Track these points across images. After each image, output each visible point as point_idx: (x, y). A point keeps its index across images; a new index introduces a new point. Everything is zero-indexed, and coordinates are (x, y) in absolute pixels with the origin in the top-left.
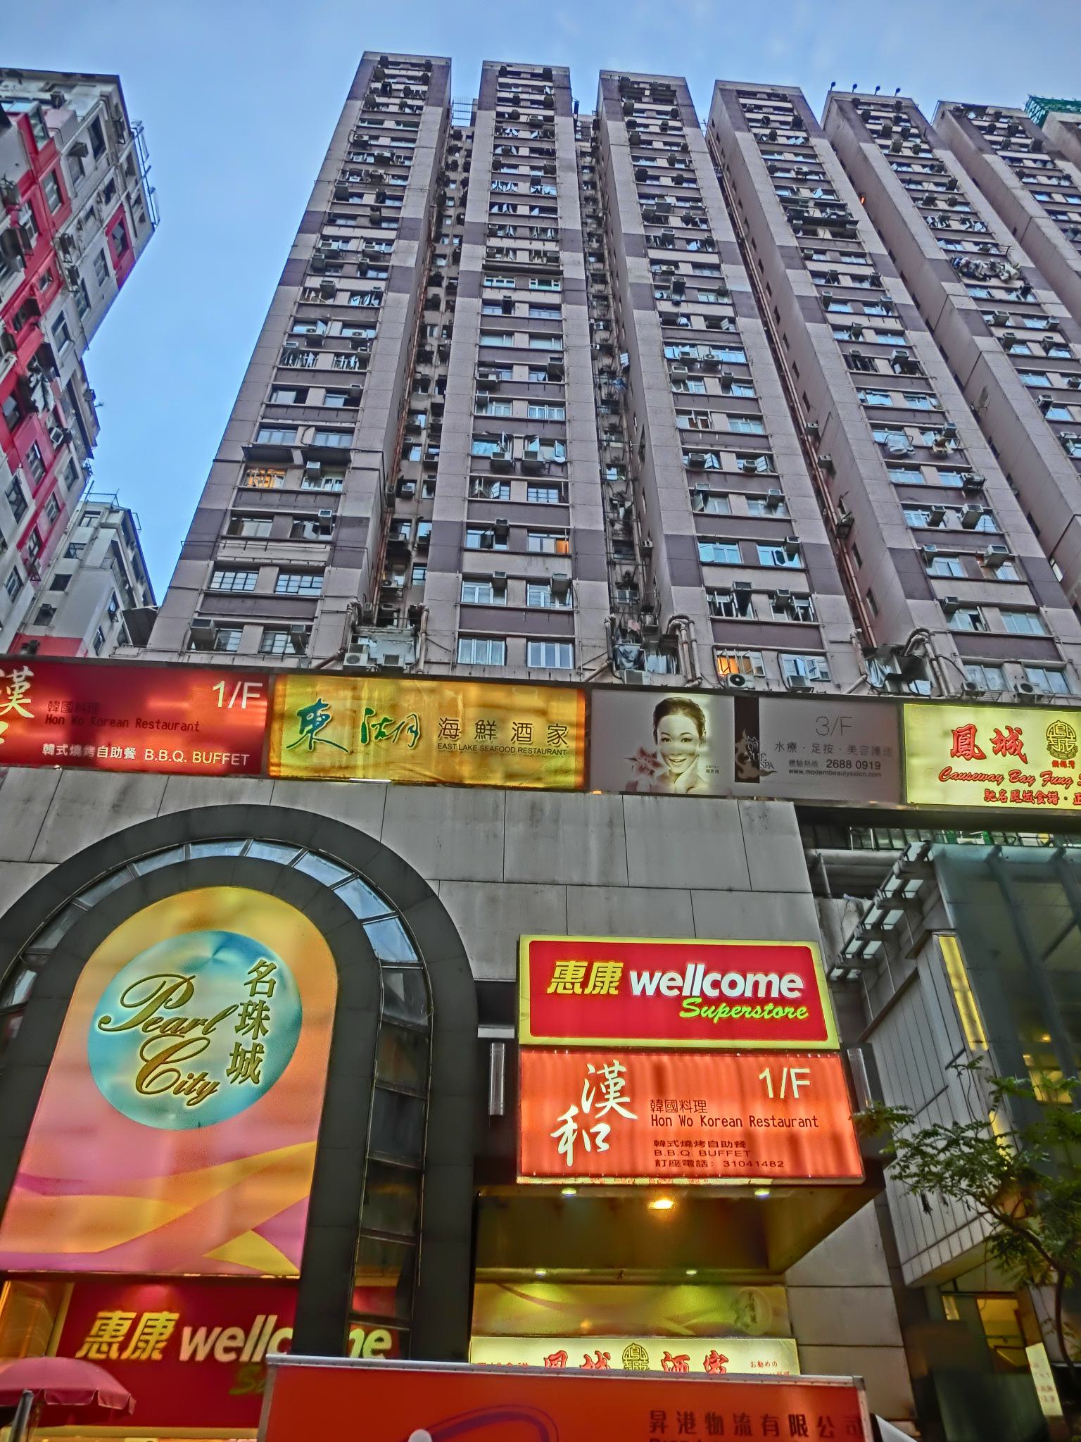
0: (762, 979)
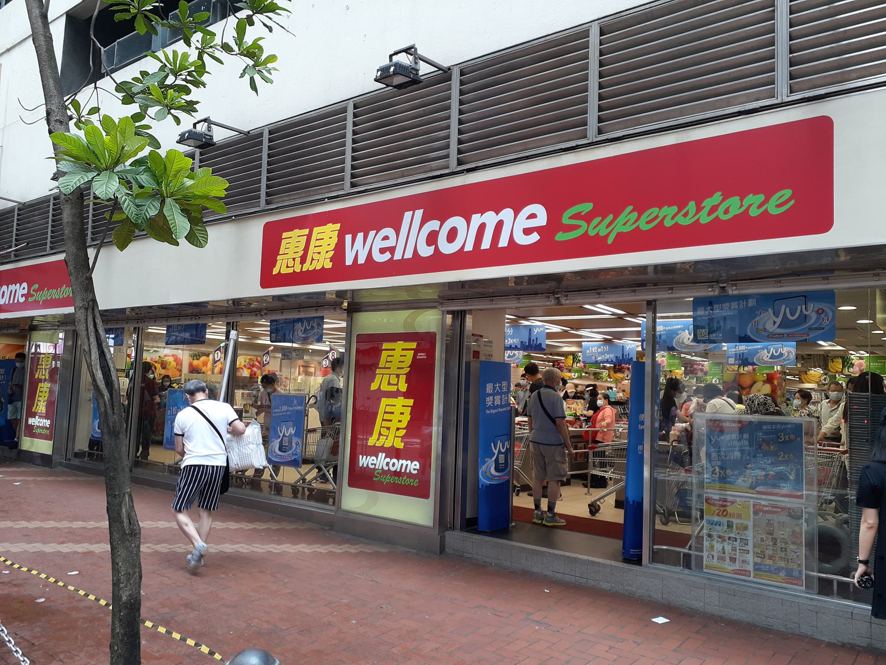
0: (490, 219)
